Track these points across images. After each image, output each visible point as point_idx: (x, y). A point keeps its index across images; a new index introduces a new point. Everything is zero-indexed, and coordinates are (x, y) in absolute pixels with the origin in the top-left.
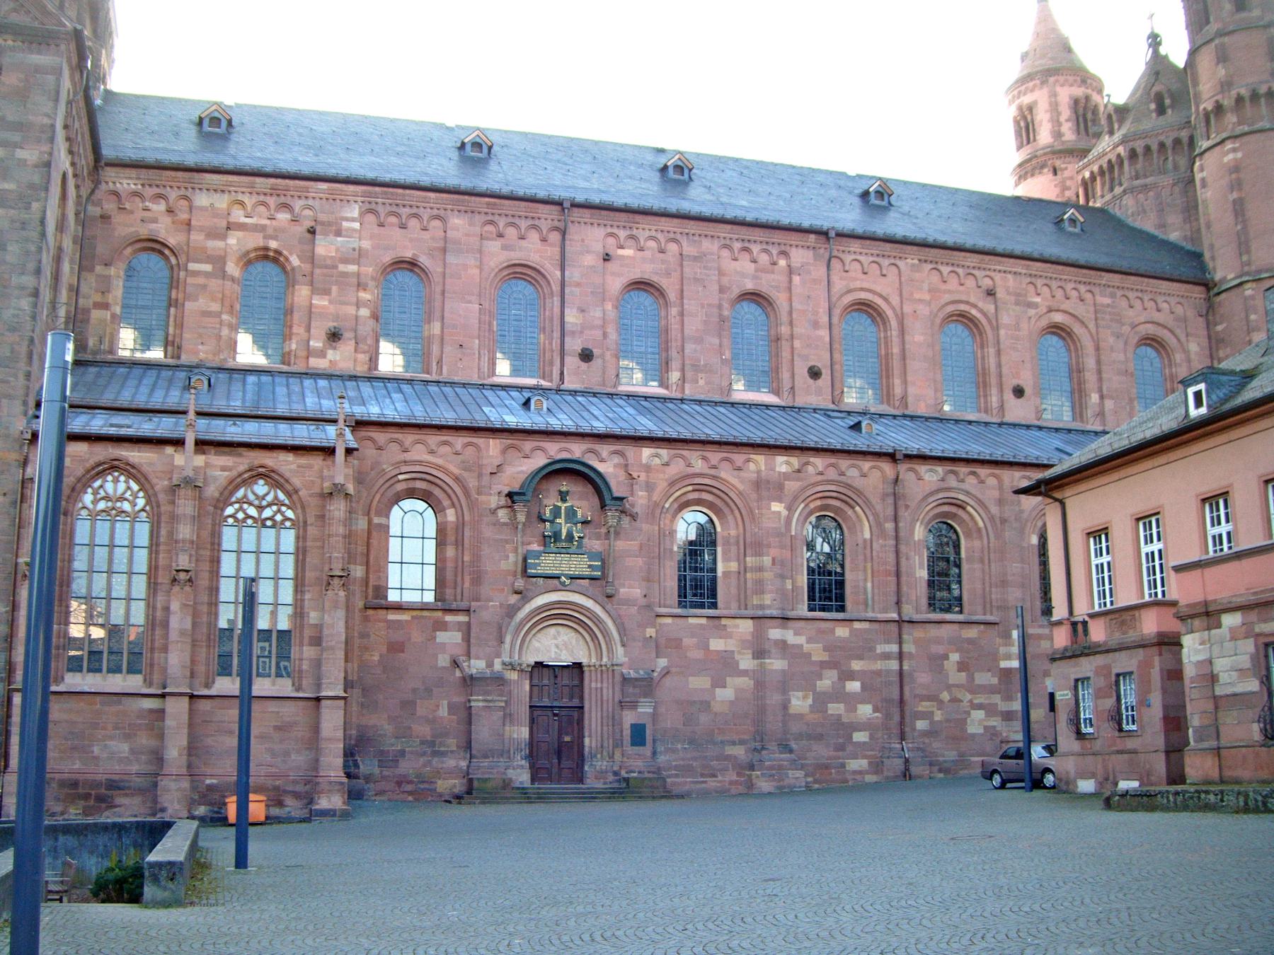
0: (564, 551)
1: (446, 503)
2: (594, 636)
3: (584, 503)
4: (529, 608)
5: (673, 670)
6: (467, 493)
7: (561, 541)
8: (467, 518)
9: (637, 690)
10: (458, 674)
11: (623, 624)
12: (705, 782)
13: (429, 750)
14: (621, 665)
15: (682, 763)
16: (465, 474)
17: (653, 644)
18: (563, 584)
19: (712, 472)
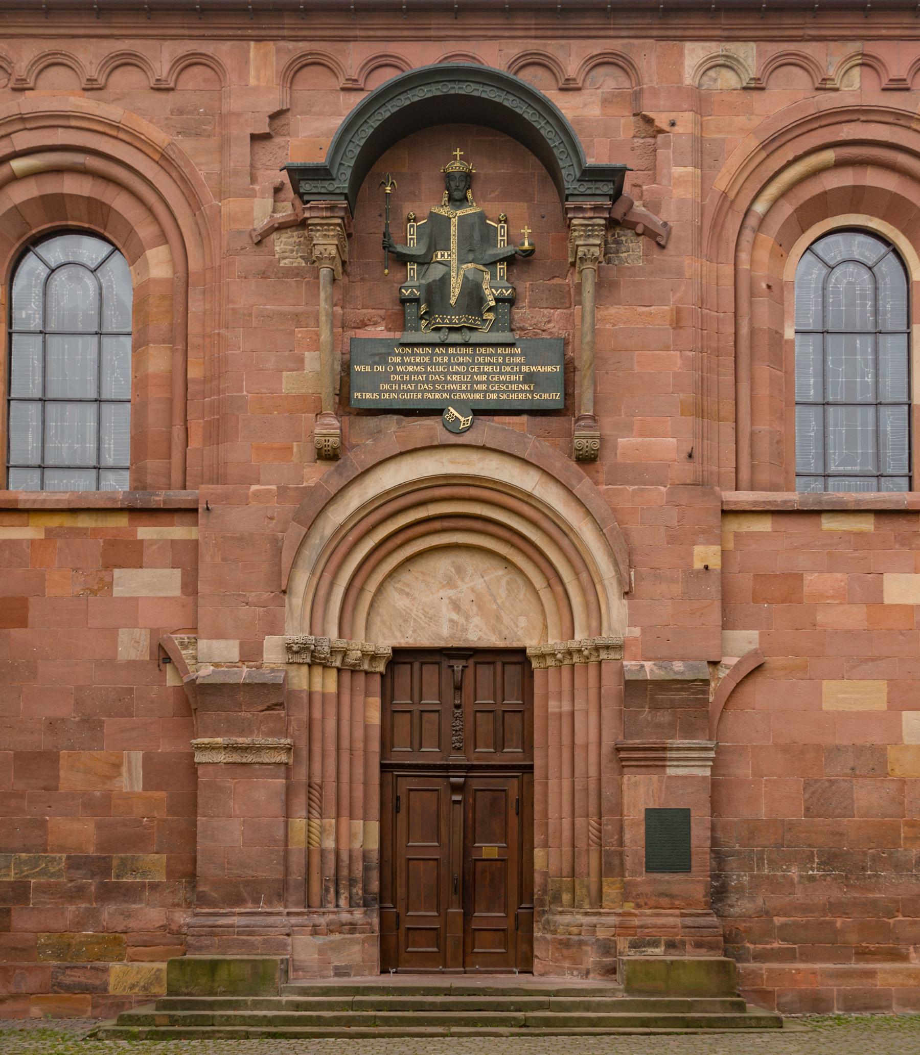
0: (455, 338)
1: (145, 231)
2: (553, 576)
3: (517, 209)
4: (355, 499)
5: (775, 661)
6: (194, 201)
7: (446, 309)
8: (194, 265)
9: (664, 717)
10: (171, 680)
11: (626, 534)
12: (871, 974)
13: (92, 885)
14: (619, 648)
15: (800, 919)
16: (186, 145)
17: (713, 589)
18: (453, 428)
19: (894, 101)
